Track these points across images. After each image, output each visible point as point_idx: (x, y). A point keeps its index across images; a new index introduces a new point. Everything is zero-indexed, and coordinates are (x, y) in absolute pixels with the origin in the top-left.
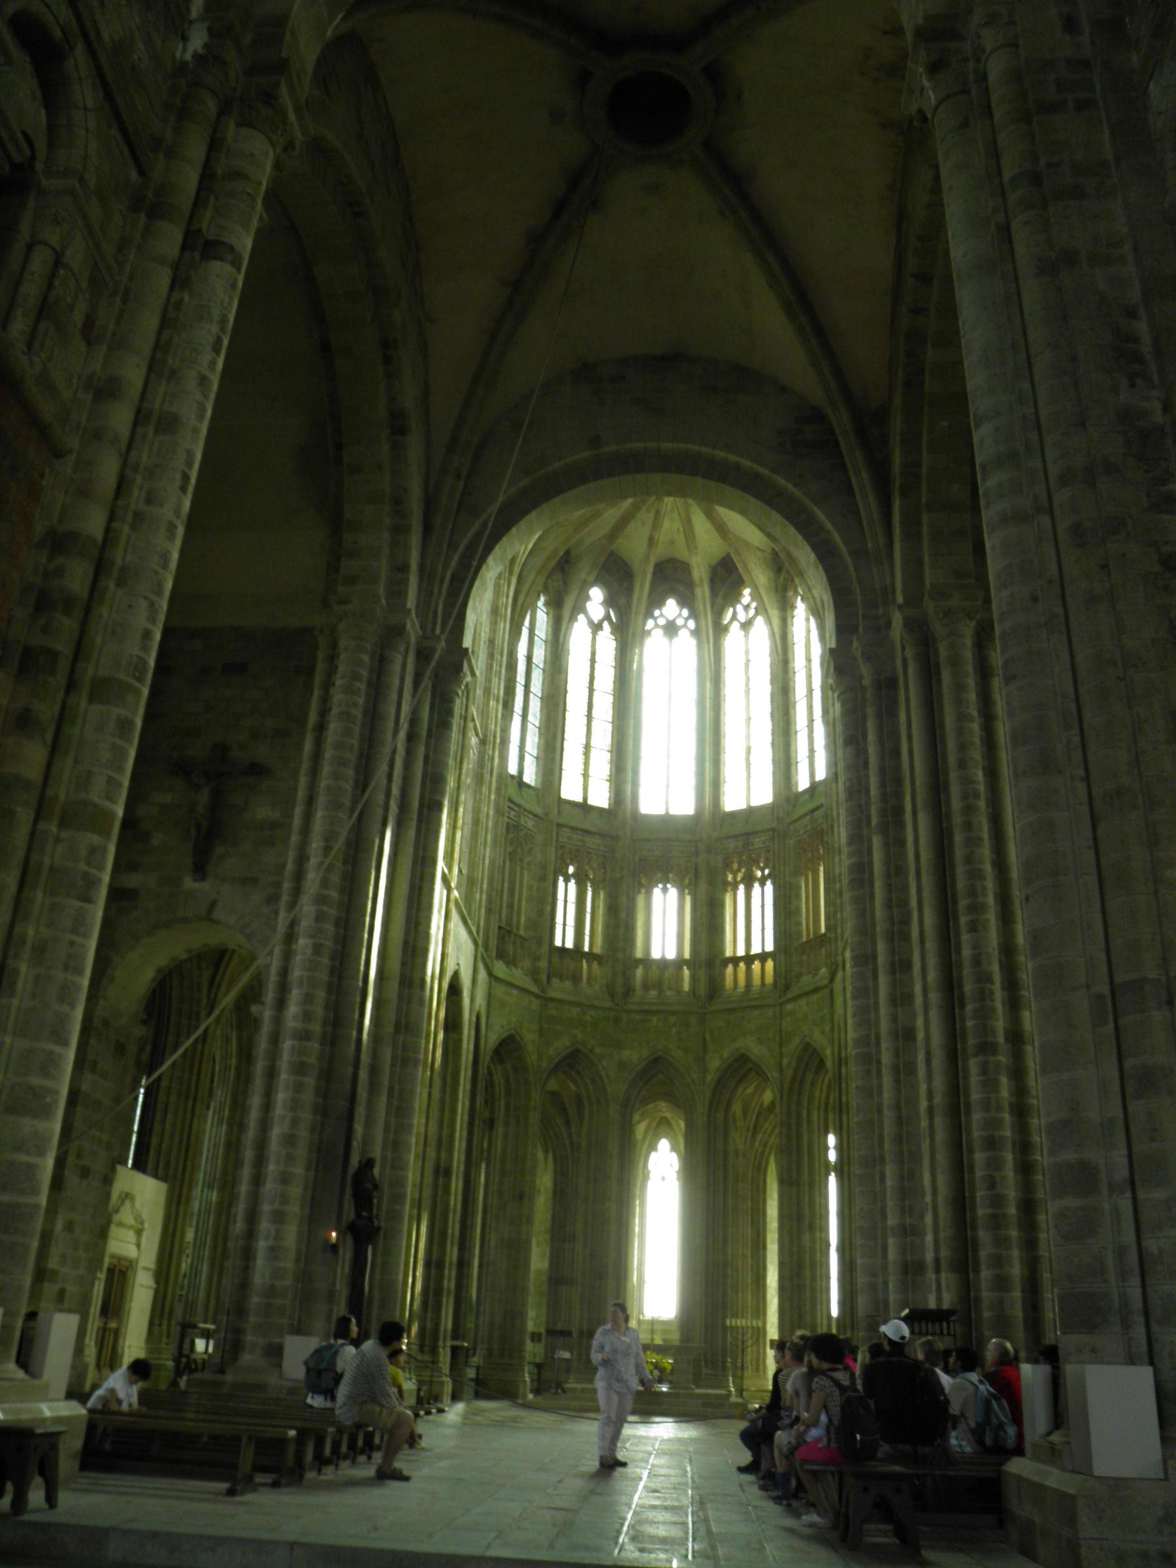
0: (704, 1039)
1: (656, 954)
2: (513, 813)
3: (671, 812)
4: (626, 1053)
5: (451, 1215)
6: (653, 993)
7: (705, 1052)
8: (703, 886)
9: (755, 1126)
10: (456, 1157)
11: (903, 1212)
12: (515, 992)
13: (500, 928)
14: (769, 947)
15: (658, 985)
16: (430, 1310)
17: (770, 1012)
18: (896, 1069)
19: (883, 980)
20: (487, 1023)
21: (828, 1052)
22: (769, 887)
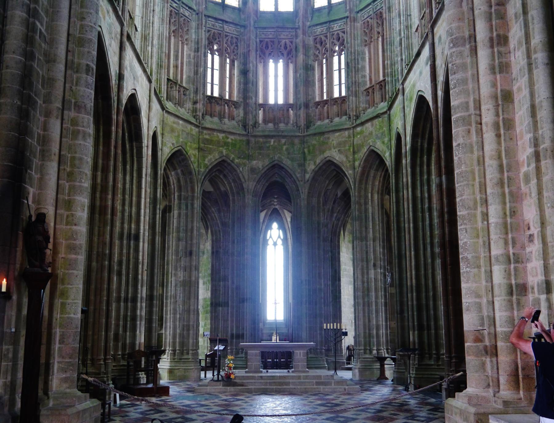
0: (304, 153)
1: (271, 101)
2: (174, 5)
3: (279, 10)
4: (254, 162)
5: (140, 266)
6: (271, 125)
7: (304, 161)
8: (301, 57)
9: (333, 208)
10: (142, 228)
11: (506, 243)
12: (181, 122)
13: (168, 79)
14: (343, 94)
15: (275, 121)
16: (128, 330)
17: (346, 133)
18: (496, 126)
19: (483, 54)
20: (162, 141)
21: (387, 154)
22: (343, 57)
